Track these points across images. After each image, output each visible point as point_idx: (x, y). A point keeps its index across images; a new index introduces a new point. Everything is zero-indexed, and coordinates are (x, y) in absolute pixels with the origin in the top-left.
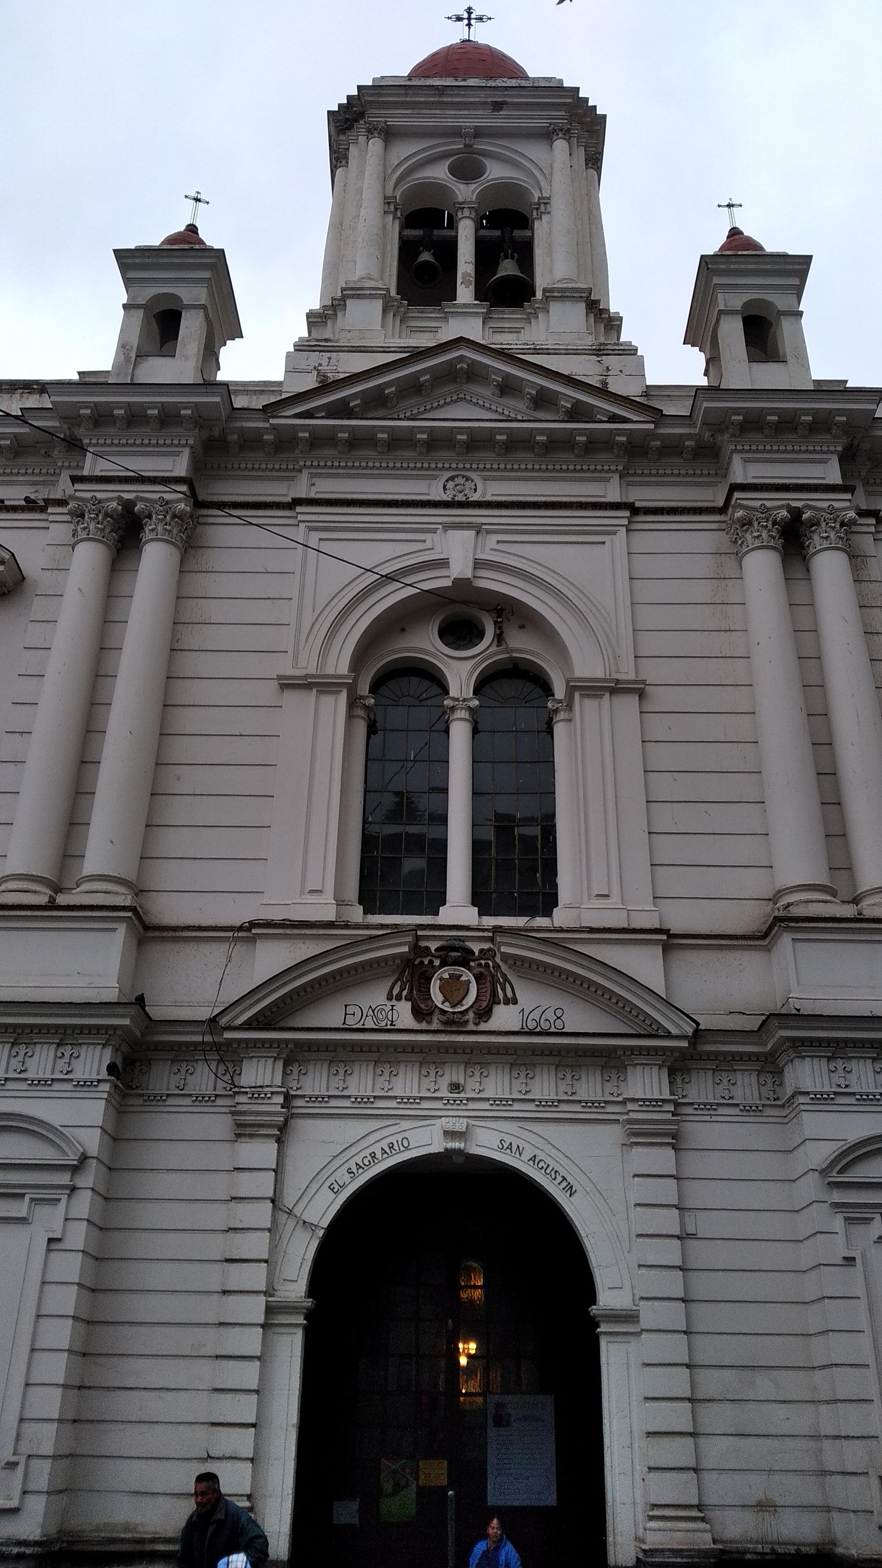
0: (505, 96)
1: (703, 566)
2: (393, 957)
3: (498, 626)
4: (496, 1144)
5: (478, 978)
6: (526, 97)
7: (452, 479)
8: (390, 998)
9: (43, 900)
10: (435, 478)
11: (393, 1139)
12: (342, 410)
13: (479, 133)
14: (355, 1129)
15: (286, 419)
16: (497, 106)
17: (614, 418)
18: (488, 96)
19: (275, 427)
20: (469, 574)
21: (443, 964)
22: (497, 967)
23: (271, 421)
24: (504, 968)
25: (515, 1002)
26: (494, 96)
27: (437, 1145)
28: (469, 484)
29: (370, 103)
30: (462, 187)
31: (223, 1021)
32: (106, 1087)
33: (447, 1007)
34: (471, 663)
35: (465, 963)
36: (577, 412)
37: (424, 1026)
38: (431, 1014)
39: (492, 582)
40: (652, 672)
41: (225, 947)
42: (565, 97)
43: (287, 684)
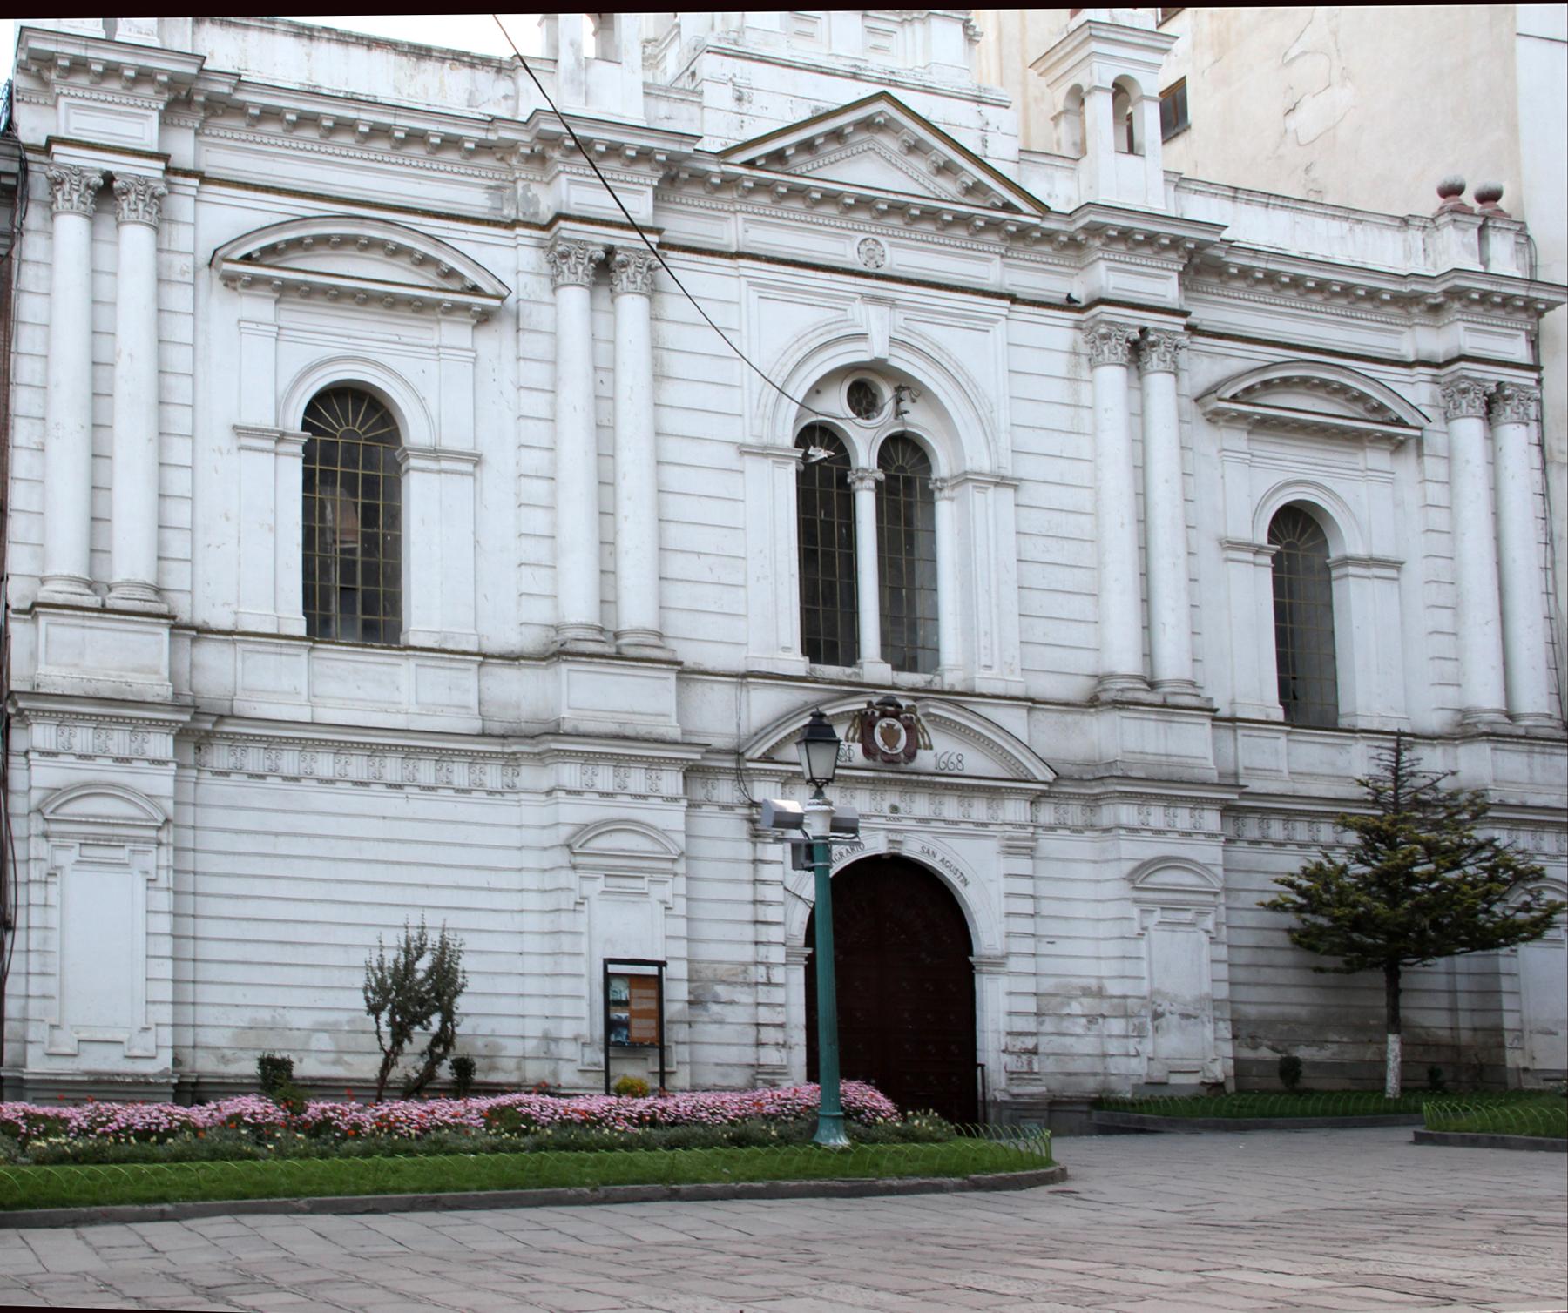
1: (1060, 365)
2: (853, 711)
3: (899, 400)
4: (918, 849)
17: (1008, 207)
19: (723, 173)
21: (884, 715)
22: (918, 720)
23: (725, 168)
24: (923, 721)
25: (931, 748)
33: (886, 749)
35: (896, 716)
36: (975, 189)
39: (903, 362)
40: (1026, 468)
43: (744, 450)
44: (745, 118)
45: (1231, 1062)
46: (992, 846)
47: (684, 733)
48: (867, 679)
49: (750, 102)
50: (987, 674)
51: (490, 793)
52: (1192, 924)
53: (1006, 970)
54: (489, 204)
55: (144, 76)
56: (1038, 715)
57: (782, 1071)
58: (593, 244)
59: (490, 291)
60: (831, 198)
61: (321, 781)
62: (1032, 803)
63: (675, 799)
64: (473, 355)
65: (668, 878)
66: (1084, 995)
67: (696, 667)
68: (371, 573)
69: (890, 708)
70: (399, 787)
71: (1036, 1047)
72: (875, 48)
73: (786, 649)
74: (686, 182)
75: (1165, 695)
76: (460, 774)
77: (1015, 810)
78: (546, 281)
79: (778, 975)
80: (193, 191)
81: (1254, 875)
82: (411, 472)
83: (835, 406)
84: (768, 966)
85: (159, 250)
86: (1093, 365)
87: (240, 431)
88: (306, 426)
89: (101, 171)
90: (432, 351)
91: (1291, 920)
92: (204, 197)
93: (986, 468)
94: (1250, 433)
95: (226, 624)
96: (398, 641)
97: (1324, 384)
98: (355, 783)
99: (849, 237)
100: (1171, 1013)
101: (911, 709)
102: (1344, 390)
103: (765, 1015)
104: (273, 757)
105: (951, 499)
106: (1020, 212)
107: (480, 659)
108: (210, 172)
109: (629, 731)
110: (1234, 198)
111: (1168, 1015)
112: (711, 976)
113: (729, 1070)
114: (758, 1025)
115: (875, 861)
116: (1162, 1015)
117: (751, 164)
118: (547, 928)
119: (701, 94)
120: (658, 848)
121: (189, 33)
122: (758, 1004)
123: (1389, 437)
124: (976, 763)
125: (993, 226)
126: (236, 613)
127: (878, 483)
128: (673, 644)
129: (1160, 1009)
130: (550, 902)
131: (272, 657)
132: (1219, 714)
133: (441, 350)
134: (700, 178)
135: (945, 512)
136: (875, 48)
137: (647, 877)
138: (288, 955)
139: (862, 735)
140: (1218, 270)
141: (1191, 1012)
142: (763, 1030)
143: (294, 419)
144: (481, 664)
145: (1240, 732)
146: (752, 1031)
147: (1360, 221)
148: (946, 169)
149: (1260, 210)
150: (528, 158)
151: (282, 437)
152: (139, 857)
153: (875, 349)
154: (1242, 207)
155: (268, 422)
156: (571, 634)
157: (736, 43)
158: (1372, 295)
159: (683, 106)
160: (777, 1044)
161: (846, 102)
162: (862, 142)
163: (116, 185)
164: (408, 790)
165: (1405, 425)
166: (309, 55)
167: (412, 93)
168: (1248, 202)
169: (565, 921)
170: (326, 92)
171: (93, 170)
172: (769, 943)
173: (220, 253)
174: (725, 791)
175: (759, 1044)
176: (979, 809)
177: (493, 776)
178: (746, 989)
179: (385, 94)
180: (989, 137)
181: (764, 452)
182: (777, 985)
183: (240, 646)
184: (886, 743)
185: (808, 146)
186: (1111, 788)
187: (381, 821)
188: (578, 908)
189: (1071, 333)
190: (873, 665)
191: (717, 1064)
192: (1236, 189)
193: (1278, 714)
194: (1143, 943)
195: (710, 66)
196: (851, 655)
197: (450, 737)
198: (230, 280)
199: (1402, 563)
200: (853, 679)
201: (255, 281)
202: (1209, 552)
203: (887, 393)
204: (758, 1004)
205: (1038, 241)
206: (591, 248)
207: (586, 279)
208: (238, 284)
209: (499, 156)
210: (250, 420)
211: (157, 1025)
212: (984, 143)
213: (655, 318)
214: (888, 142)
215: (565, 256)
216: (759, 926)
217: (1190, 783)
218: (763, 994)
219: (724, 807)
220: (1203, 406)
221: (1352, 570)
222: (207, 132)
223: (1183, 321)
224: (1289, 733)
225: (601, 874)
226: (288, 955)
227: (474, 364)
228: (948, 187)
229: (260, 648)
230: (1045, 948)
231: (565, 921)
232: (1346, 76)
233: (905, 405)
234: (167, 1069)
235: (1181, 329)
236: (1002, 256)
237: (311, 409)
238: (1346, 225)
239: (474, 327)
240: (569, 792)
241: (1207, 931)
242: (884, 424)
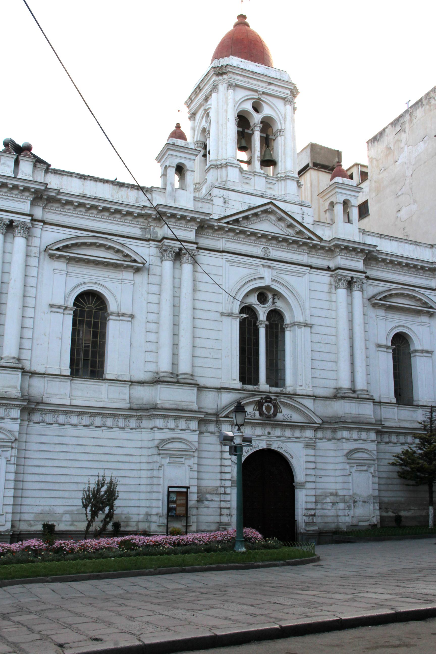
0: (273, 81)
1: (326, 288)
2: (256, 400)
3: (274, 299)
6: (280, 83)
8: (254, 410)
13: (264, 93)
16: (270, 84)
17: (310, 238)
18: (268, 79)
19: (219, 225)
21: (266, 402)
22: (278, 403)
23: (219, 224)
24: (279, 404)
29: (230, 71)
33: (267, 413)
35: (270, 402)
36: (300, 232)
40: (314, 321)
42: (291, 86)
43: (222, 314)
44: (227, 208)
45: (379, 517)
46: (301, 445)
47: (199, 408)
48: (261, 390)
49: (228, 204)
50: (301, 388)
51: (131, 429)
52: (366, 471)
53: (305, 487)
54: (141, 233)
55: (26, 189)
56: (317, 401)
57: (228, 524)
58: (175, 247)
59: (140, 261)
60: (253, 234)
61: (72, 425)
62: (314, 431)
63: (194, 431)
64: (133, 282)
65: (191, 458)
66: (331, 495)
67: (204, 386)
68: (94, 354)
69: (268, 399)
70: (100, 427)
71: (315, 513)
72: (269, 188)
73: (234, 380)
74: (206, 228)
75: (358, 395)
76: (121, 422)
77: (309, 433)
78: (159, 259)
79: (228, 491)
80: (41, 227)
81: (387, 454)
82: (110, 321)
83: (253, 300)
84: (225, 487)
85: (28, 246)
86: (336, 288)
87: (51, 306)
88: (75, 304)
89: (9, 219)
90: (120, 281)
91: (397, 468)
92: (44, 229)
93: (302, 321)
94: (385, 310)
95: (42, 371)
96: (102, 377)
97: (408, 295)
98: (84, 426)
99: (259, 247)
100: (359, 501)
101: (275, 400)
102: (414, 297)
103: (223, 505)
104: (56, 417)
105: (290, 331)
106: (313, 240)
107: (130, 383)
108: (47, 220)
109: (180, 408)
110: (380, 237)
111: (358, 502)
112: (205, 491)
113: (210, 524)
114: (221, 508)
115: (262, 450)
116: (356, 502)
117: (228, 223)
118: (149, 475)
119: (213, 200)
120: (188, 447)
121: (43, 176)
122: (221, 501)
123: (428, 312)
124: (296, 417)
125: (305, 244)
126: (46, 367)
127: (266, 325)
128: (196, 378)
129: (356, 500)
130: (150, 466)
131: (58, 383)
132: (375, 401)
133: (122, 280)
134: (211, 227)
135: (288, 335)
136: (269, 188)
137: (184, 457)
138: (57, 487)
139: (259, 408)
140: (376, 259)
141: (366, 500)
142: (222, 510)
143: (71, 302)
144: (131, 385)
145: (382, 406)
146: (219, 510)
147: (419, 245)
148: (290, 226)
149: (388, 241)
150: (155, 219)
151: (66, 308)
152: (4, 453)
153: (267, 282)
154: (383, 240)
155: (61, 303)
156: (162, 375)
157: (224, 185)
158: (423, 268)
159: (207, 204)
160: (227, 515)
161: (259, 204)
162: (264, 217)
163: (14, 224)
164: (103, 428)
165: (433, 308)
166: (83, 184)
167: (117, 197)
168: (385, 239)
169: (155, 473)
170: (88, 196)
171: (6, 219)
172: (225, 480)
173: (49, 247)
174: (212, 428)
175: (221, 515)
176: (297, 433)
177: (133, 423)
178: (217, 496)
179: (108, 197)
180: (304, 216)
181: (229, 315)
182: (228, 494)
183: (46, 379)
184: (267, 411)
185: (246, 218)
186: (340, 426)
187: (93, 439)
188: (160, 468)
189: (330, 278)
190: (263, 385)
191: (206, 522)
192: (381, 235)
193: (394, 400)
194: (350, 478)
195: (216, 192)
196: (256, 381)
197: (119, 410)
198: (52, 256)
199: (433, 352)
200: (257, 390)
201: (60, 257)
202: (372, 347)
203: (270, 296)
204: (221, 501)
205: (319, 249)
206: (174, 248)
207: (172, 258)
208: (54, 257)
209: (145, 218)
210: (56, 302)
211: (6, 513)
212: (303, 218)
213: (194, 271)
215: (165, 251)
216: (222, 474)
217: (366, 423)
218: (223, 497)
219: (212, 433)
220: (371, 302)
221: (417, 354)
222: (47, 208)
223: (364, 275)
224: (398, 407)
225: (168, 456)
226: (57, 487)
227: (133, 285)
228: (291, 232)
229: (54, 379)
230: (319, 480)
231: (155, 473)
232: (415, 201)
233: (276, 300)
234: (9, 529)
235: (364, 277)
236: (308, 254)
237: (77, 299)
238: (414, 246)
239: (134, 273)
240: (158, 428)
241: (371, 473)
242: (269, 306)
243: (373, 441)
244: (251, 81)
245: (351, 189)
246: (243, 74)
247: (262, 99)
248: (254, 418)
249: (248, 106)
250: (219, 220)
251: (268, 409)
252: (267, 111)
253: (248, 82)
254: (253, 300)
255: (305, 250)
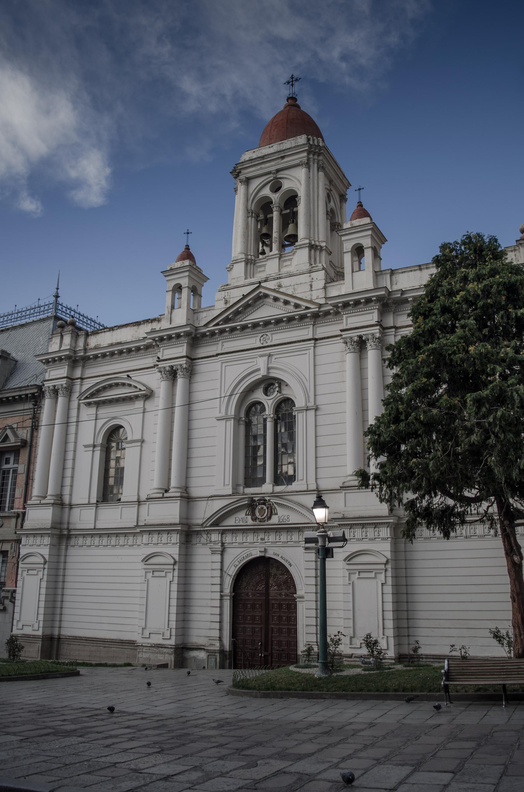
2: (245, 504)
5: (268, 508)
7: (262, 336)
8: (246, 515)
9: (161, 495)
10: (257, 336)
11: (248, 553)
12: (227, 320)
13: (278, 171)
14: (239, 550)
15: (211, 328)
16: (283, 158)
17: (307, 308)
18: (279, 155)
19: (209, 331)
20: (265, 374)
21: (259, 504)
25: (277, 514)
26: (281, 154)
27: (259, 554)
28: (267, 337)
29: (241, 169)
30: (274, 195)
31: (204, 525)
32: (178, 544)
33: (260, 517)
34: (272, 400)
35: (264, 504)
37: (254, 522)
38: (256, 519)
39: (274, 374)
41: (206, 502)
60: (255, 325)
110: (420, 269)
117: (217, 324)
119: (214, 306)
125: (303, 317)
134: (204, 335)
148: (286, 303)
153: (263, 372)
192: (420, 266)
214: (270, 300)
217: (375, 517)
228: (291, 308)
243: (384, 539)
244: (263, 166)
245: (359, 230)
246: (253, 164)
247: (278, 176)
248: (246, 524)
249: (267, 192)
250: (206, 325)
251: (261, 511)
252: (286, 185)
253: (261, 168)
254: (259, 395)
255: (309, 322)
